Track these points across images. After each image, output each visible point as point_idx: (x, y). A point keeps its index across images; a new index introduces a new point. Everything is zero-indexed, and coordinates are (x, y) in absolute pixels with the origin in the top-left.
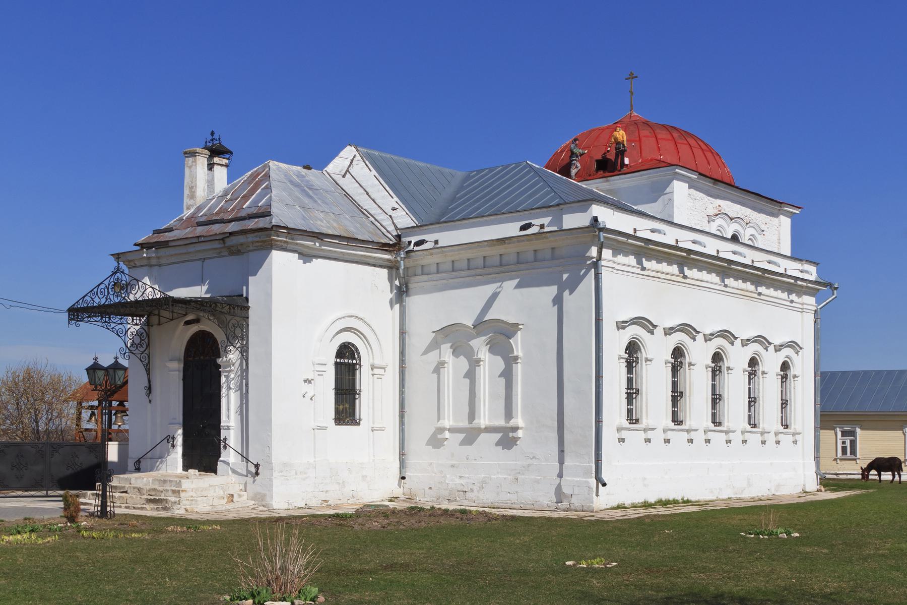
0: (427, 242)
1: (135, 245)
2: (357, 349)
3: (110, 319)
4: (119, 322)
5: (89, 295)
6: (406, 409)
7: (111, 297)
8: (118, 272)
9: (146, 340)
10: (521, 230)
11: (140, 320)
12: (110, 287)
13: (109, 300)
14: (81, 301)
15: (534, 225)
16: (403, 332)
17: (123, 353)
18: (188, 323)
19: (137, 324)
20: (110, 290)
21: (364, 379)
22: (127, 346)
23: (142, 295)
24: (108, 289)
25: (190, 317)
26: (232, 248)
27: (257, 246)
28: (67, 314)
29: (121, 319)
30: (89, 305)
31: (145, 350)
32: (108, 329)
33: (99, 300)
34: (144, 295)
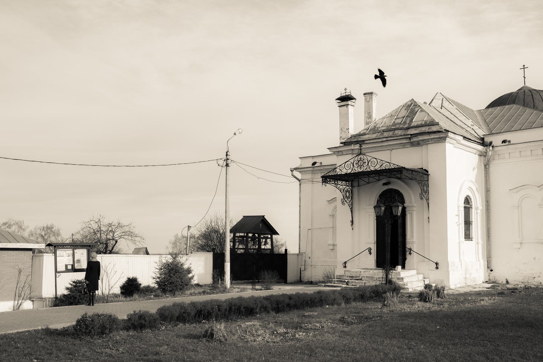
3: (338, 183)
4: (341, 184)
7: (356, 169)
8: (361, 155)
11: (349, 183)
12: (355, 163)
17: (342, 201)
18: (385, 184)
19: (347, 186)
20: (355, 165)
24: (353, 165)
26: (414, 143)
27: (435, 141)
31: (351, 200)
32: (337, 188)
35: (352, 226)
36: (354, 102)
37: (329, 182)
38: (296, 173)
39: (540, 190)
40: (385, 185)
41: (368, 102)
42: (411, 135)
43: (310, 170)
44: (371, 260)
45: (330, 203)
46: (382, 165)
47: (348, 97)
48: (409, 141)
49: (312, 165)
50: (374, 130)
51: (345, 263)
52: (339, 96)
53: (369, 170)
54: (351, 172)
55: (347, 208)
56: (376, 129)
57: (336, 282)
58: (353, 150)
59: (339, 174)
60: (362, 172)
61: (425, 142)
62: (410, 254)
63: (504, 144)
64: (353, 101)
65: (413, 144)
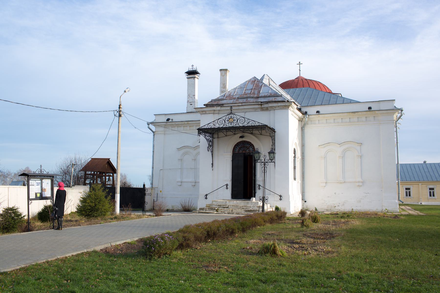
7: (227, 124)
8: (231, 114)
12: (226, 120)
14: (206, 126)
20: (226, 121)
24: (225, 122)
26: (263, 108)
28: (198, 131)
35: (212, 167)
36: (198, 76)
38: (151, 126)
39: (340, 147)
40: (241, 138)
41: (223, 76)
42: (261, 102)
43: (164, 125)
44: (228, 193)
45: (179, 150)
46: (249, 122)
47: (195, 72)
48: (260, 107)
49: (167, 121)
50: (230, 97)
51: (206, 195)
52: (187, 71)
53: (238, 126)
54: (223, 127)
55: (210, 153)
56: (231, 96)
57: (208, 210)
58: (214, 110)
59: (212, 127)
60: (232, 127)
61: (274, 108)
62: (259, 189)
63: (318, 114)
64: (198, 75)
65: (262, 109)
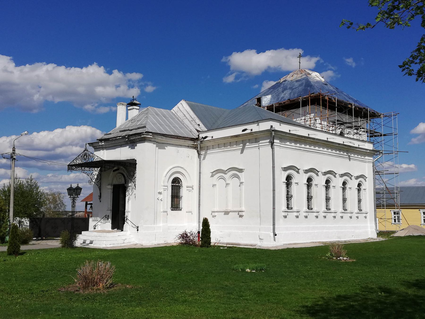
0: (208, 137)
1: (97, 140)
2: (180, 180)
3: (85, 169)
5: (75, 159)
6: (201, 204)
9: (100, 177)
10: (242, 132)
11: (97, 169)
12: (83, 156)
13: (82, 161)
14: (72, 162)
15: (248, 129)
16: (200, 173)
19: (96, 171)
20: (83, 158)
21: (184, 192)
22: (91, 180)
23: (94, 160)
25: (115, 168)
29: (90, 169)
30: (75, 164)
31: (99, 181)
33: (79, 162)
34: (94, 159)
35: (100, 199)
37: (75, 169)
53: (89, 161)
